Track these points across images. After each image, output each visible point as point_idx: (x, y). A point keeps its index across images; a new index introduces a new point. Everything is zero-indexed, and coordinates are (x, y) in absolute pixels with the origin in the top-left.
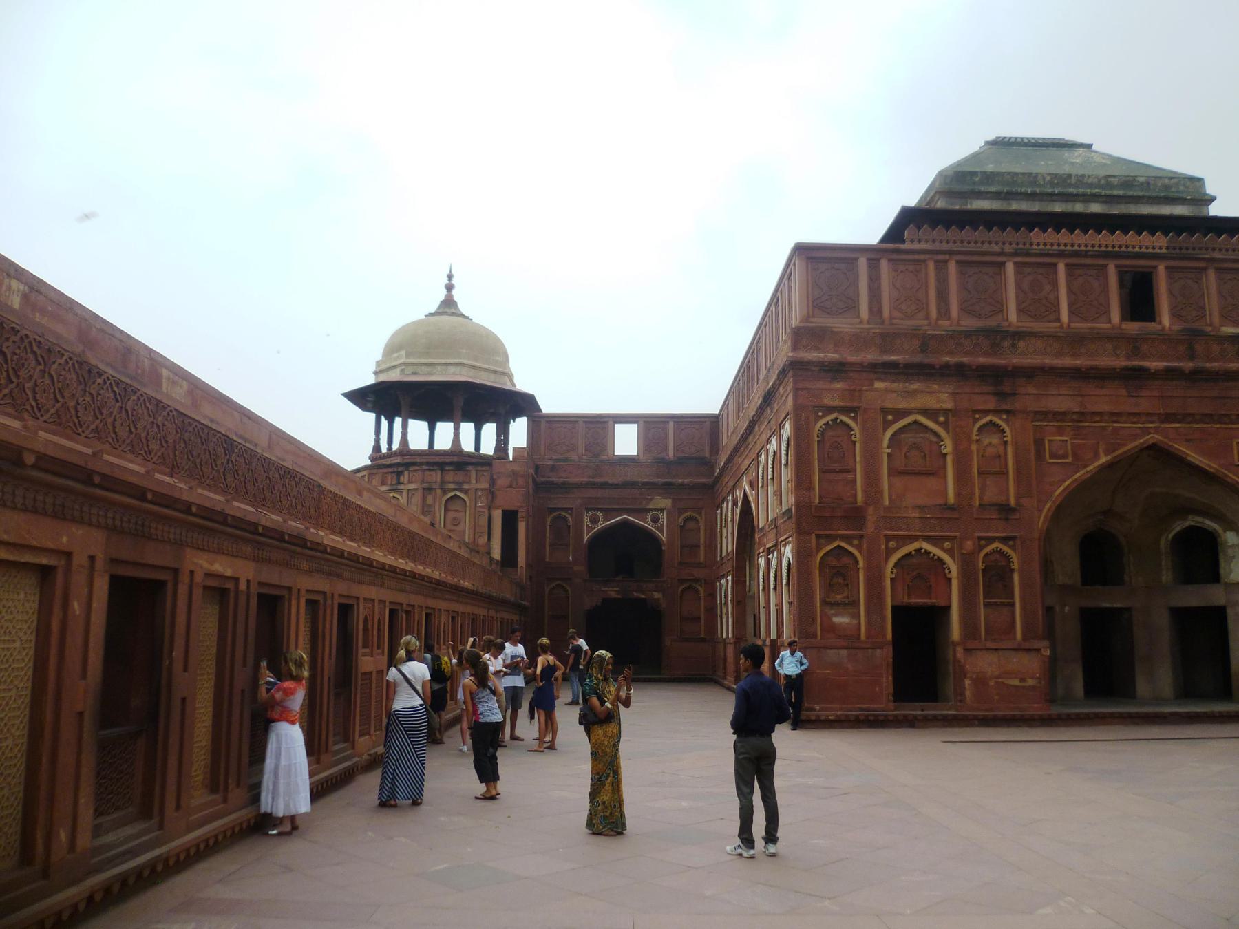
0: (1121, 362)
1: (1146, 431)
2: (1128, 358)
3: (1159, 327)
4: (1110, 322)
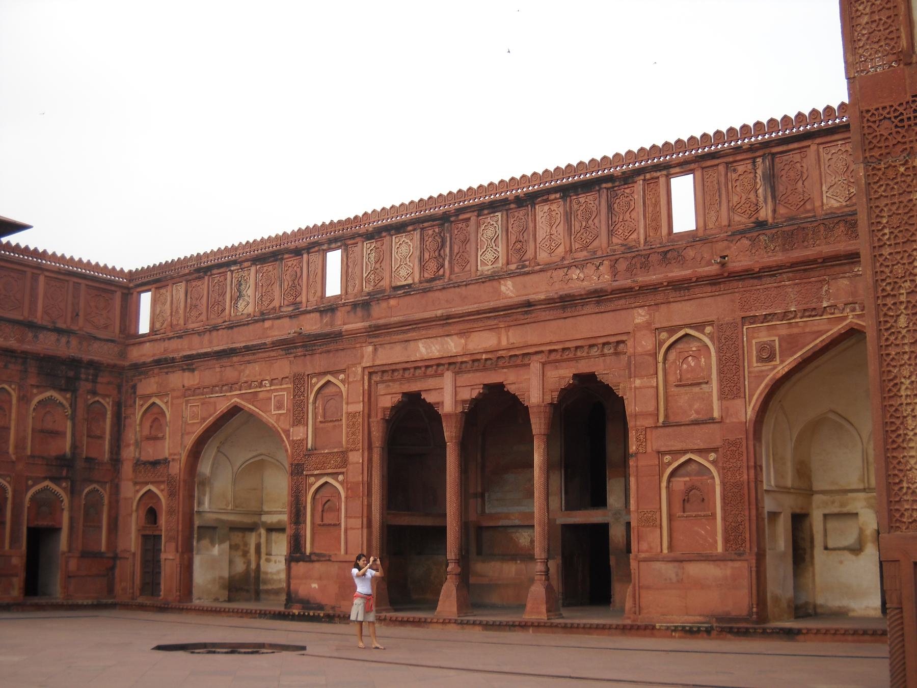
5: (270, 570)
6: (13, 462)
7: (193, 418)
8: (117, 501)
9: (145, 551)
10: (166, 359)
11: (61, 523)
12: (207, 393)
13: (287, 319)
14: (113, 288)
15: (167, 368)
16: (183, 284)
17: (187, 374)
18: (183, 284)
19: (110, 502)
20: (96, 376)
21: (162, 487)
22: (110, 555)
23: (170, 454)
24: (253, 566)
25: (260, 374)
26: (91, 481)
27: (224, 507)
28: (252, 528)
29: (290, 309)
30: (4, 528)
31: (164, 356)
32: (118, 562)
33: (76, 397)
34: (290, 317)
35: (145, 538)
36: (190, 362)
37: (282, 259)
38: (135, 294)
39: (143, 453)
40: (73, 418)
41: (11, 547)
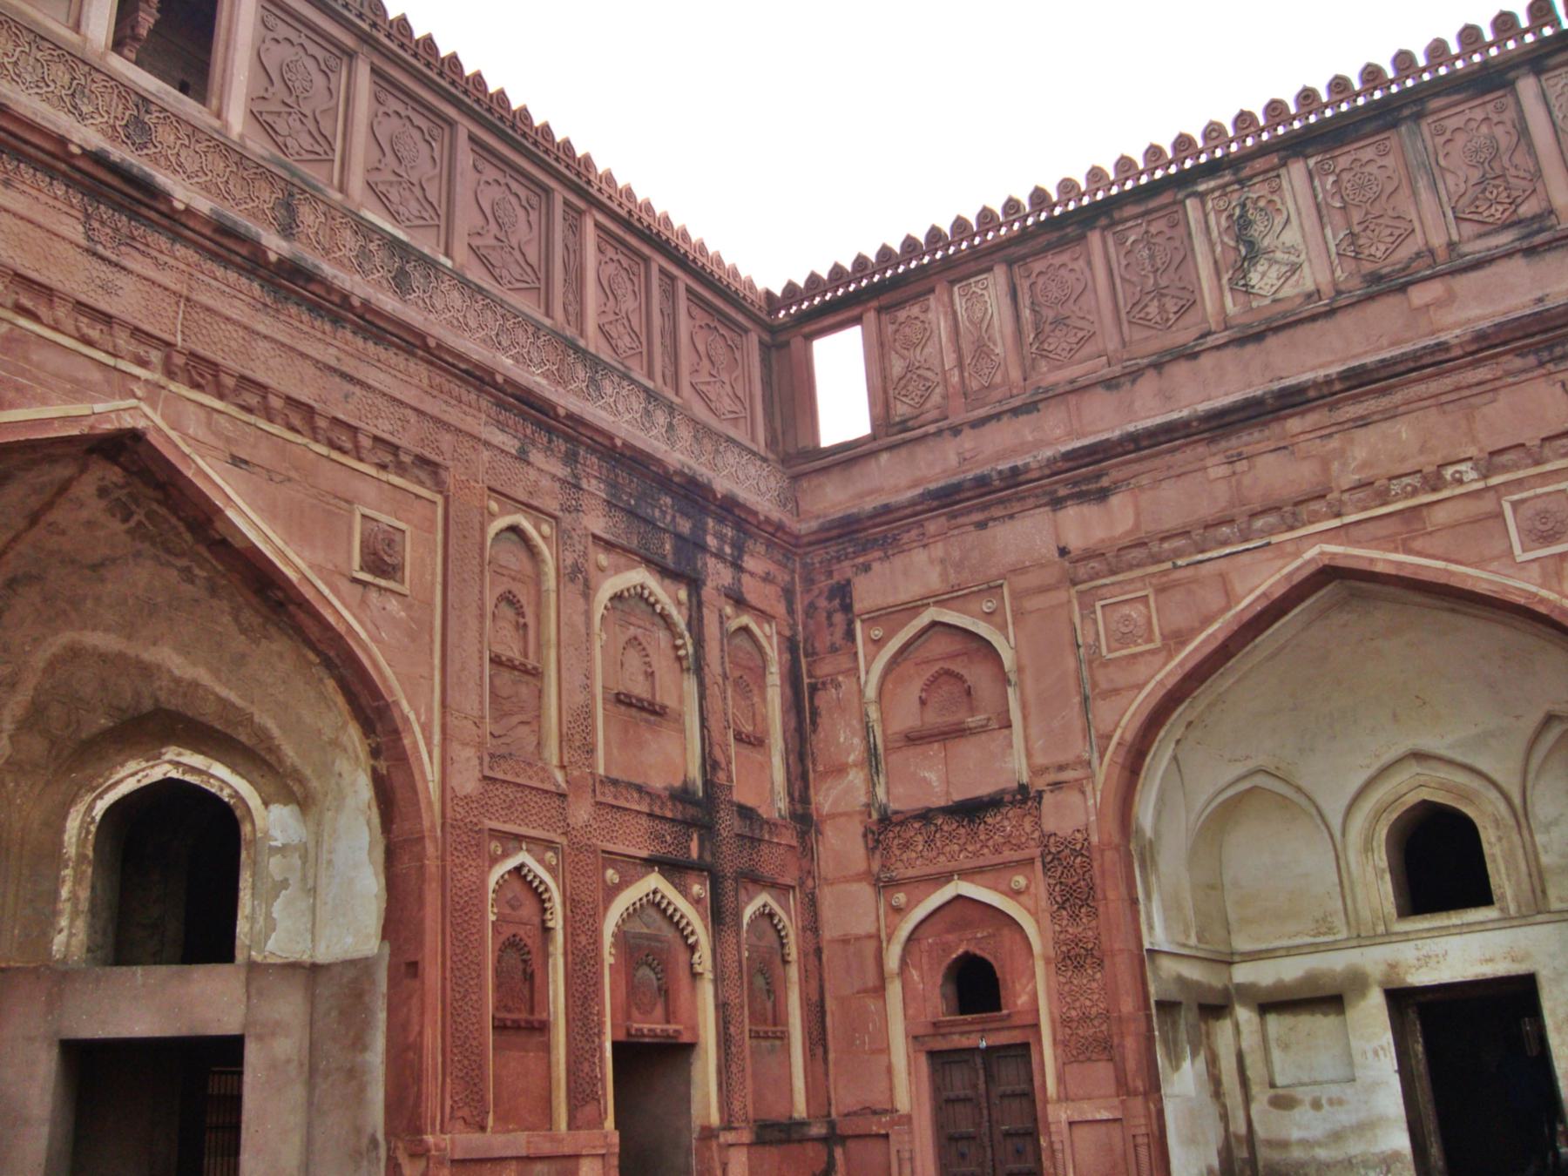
0: (86, 135)
1: (121, 384)
2: (112, 134)
3: (217, 123)
4: (77, 27)
5: (1295, 1134)
6: (563, 796)
7: (1125, 639)
8: (818, 951)
9: (943, 1104)
10: (982, 482)
11: (694, 1029)
12: (1178, 553)
13: (1518, 262)
14: (740, 318)
15: (985, 507)
16: (1000, 272)
17: (1071, 512)
18: (999, 276)
19: (803, 954)
20: (739, 548)
21: (1020, 881)
22: (818, 1130)
23: (1037, 771)
24: (1239, 1127)
25: (1422, 450)
26: (754, 879)
27: (1182, 939)
28: (1215, 1008)
29: (1504, 239)
30: (547, 1048)
31: (970, 475)
32: (838, 1153)
33: (700, 604)
34: (1530, 252)
35: (941, 1060)
36: (1085, 473)
37: (1418, 116)
38: (797, 342)
39: (899, 790)
40: (699, 668)
41: (572, 1124)
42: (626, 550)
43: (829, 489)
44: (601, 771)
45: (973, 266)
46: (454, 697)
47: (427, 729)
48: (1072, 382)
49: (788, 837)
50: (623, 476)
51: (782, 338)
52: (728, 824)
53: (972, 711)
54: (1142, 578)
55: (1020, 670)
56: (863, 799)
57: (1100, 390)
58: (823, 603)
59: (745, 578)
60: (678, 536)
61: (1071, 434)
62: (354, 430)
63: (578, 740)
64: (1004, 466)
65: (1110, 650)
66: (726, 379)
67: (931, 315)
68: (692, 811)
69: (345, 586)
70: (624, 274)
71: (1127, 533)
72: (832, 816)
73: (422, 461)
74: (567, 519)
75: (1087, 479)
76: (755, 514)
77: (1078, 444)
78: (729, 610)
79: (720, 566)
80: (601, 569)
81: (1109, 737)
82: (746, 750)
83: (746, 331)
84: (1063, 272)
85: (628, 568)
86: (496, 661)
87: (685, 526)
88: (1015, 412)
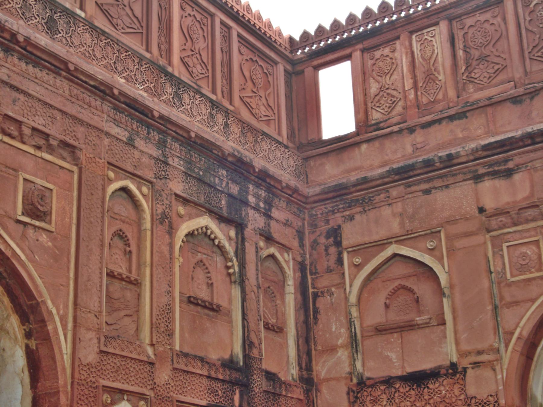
6: (152, 364)
7: (522, 269)
10: (428, 164)
14: (272, 55)
15: (429, 180)
16: (443, 26)
17: (487, 184)
18: (442, 29)
20: (269, 204)
23: (463, 354)
31: (420, 159)
33: (243, 240)
38: (309, 71)
39: (371, 364)
42: (196, 204)
43: (328, 167)
44: (177, 348)
45: (426, 22)
46: (82, 297)
47: (64, 320)
48: (490, 98)
49: (298, 393)
50: (195, 157)
51: (299, 68)
52: (259, 384)
53: (420, 313)
54: (535, 229)
55: (452, 287)
56: (348, 369)
57: (508, 104)
58: (322, 240)
59: (273, 223)
60: (230, 196)
61: (488, 133)
62: (19, 123)
63: (163, 326)
64: (443, 153)
65: (512, 276)
66: (262, 94)
67: (397, 54)
68: (236, 375)
69: (11, 225)
70: (197, 24)
71: (527, 198)
72: (327, 380)
73: (64, 144)
74: (159, 184)
75: (498, 163)
76: (280, 182)
77: (492, 140)
78: (262, 244)
79: (257, 215)
80: (180, 216)
81: (512, 334)
82: (271, 335)
83: (276, 63)
84: (486, 25)
85: (198, 216)
86: (111, 275)
87: (235, 189)
88: (451, 118)
